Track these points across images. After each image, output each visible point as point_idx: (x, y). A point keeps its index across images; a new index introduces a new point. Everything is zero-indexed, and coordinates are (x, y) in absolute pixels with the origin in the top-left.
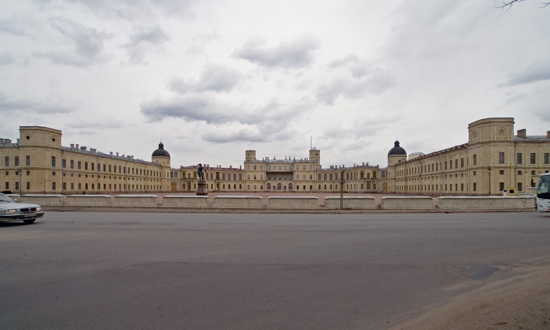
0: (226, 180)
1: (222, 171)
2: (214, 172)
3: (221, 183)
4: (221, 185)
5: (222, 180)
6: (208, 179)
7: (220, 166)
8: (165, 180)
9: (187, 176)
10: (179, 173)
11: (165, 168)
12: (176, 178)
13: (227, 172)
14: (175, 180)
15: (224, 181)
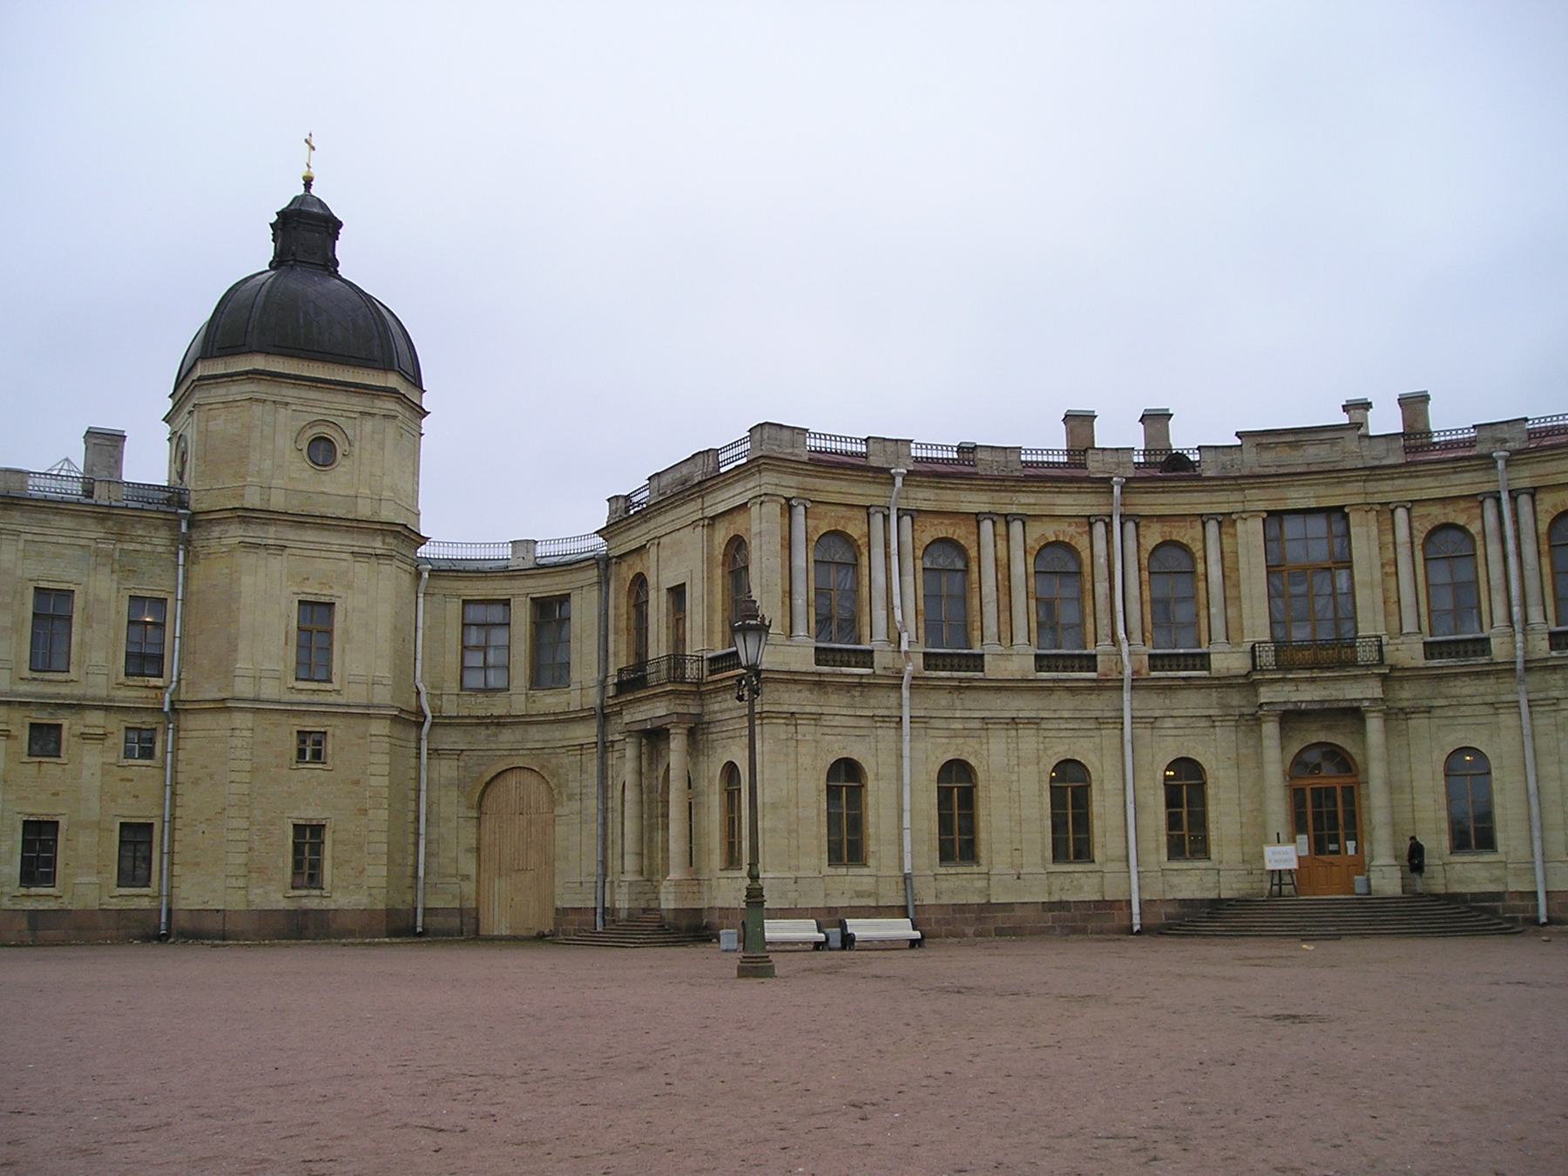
0: (1499, 649)
1: (1387, 490)
2: (1225, 521)
3: (1374, 725)
4: (1376, 771)
5: (1409, 653)
6: (1090, 662)
7: (1414, 405)
8: (222, 719)
9: (658, 647)
10: (583, 612)
11: (235, 533)
12: (550, 701)
13: (1524, 477)
14: (536, 737)
15: (1465, 688)
